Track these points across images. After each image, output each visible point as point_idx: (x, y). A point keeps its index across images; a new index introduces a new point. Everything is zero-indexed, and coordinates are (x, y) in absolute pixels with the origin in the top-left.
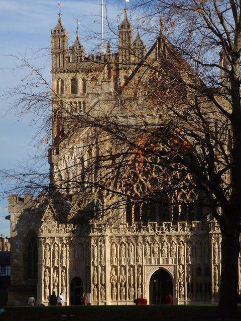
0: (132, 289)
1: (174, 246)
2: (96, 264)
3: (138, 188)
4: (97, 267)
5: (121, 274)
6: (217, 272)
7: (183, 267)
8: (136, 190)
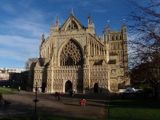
0: (60, 86)
1: (73, 73)
2: (49, 79)
3: (64, 56)
4: (49, 80)
5: (56, 82)
6: (85, 82)
7: (75, 80)
8: (63, 57)
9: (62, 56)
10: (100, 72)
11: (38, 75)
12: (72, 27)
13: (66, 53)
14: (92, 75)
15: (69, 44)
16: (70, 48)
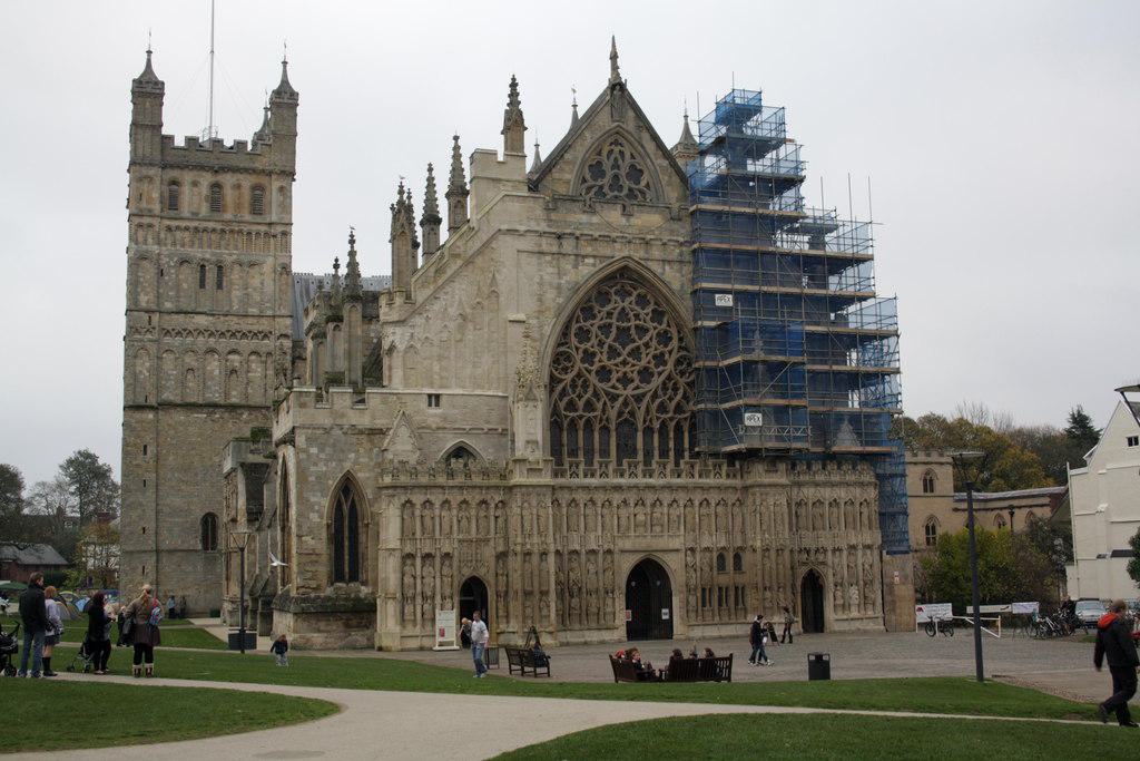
3: (574, 385)
9: (561, 381)
10: (830, 504)
11: (428, 522)
12: (616, 177)
13: (592, 364)
14: (790, 523)
15: (603, 297)
16: (614, 330)
